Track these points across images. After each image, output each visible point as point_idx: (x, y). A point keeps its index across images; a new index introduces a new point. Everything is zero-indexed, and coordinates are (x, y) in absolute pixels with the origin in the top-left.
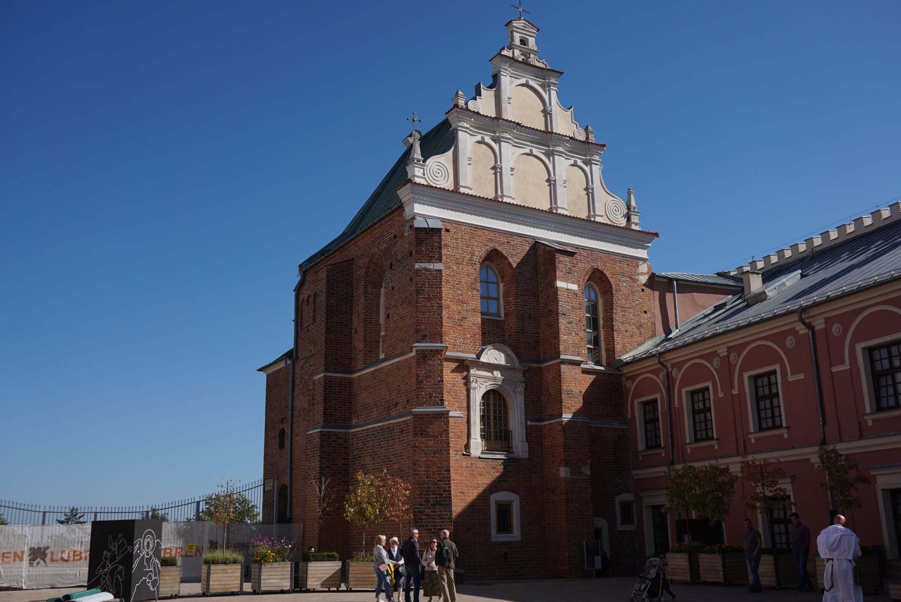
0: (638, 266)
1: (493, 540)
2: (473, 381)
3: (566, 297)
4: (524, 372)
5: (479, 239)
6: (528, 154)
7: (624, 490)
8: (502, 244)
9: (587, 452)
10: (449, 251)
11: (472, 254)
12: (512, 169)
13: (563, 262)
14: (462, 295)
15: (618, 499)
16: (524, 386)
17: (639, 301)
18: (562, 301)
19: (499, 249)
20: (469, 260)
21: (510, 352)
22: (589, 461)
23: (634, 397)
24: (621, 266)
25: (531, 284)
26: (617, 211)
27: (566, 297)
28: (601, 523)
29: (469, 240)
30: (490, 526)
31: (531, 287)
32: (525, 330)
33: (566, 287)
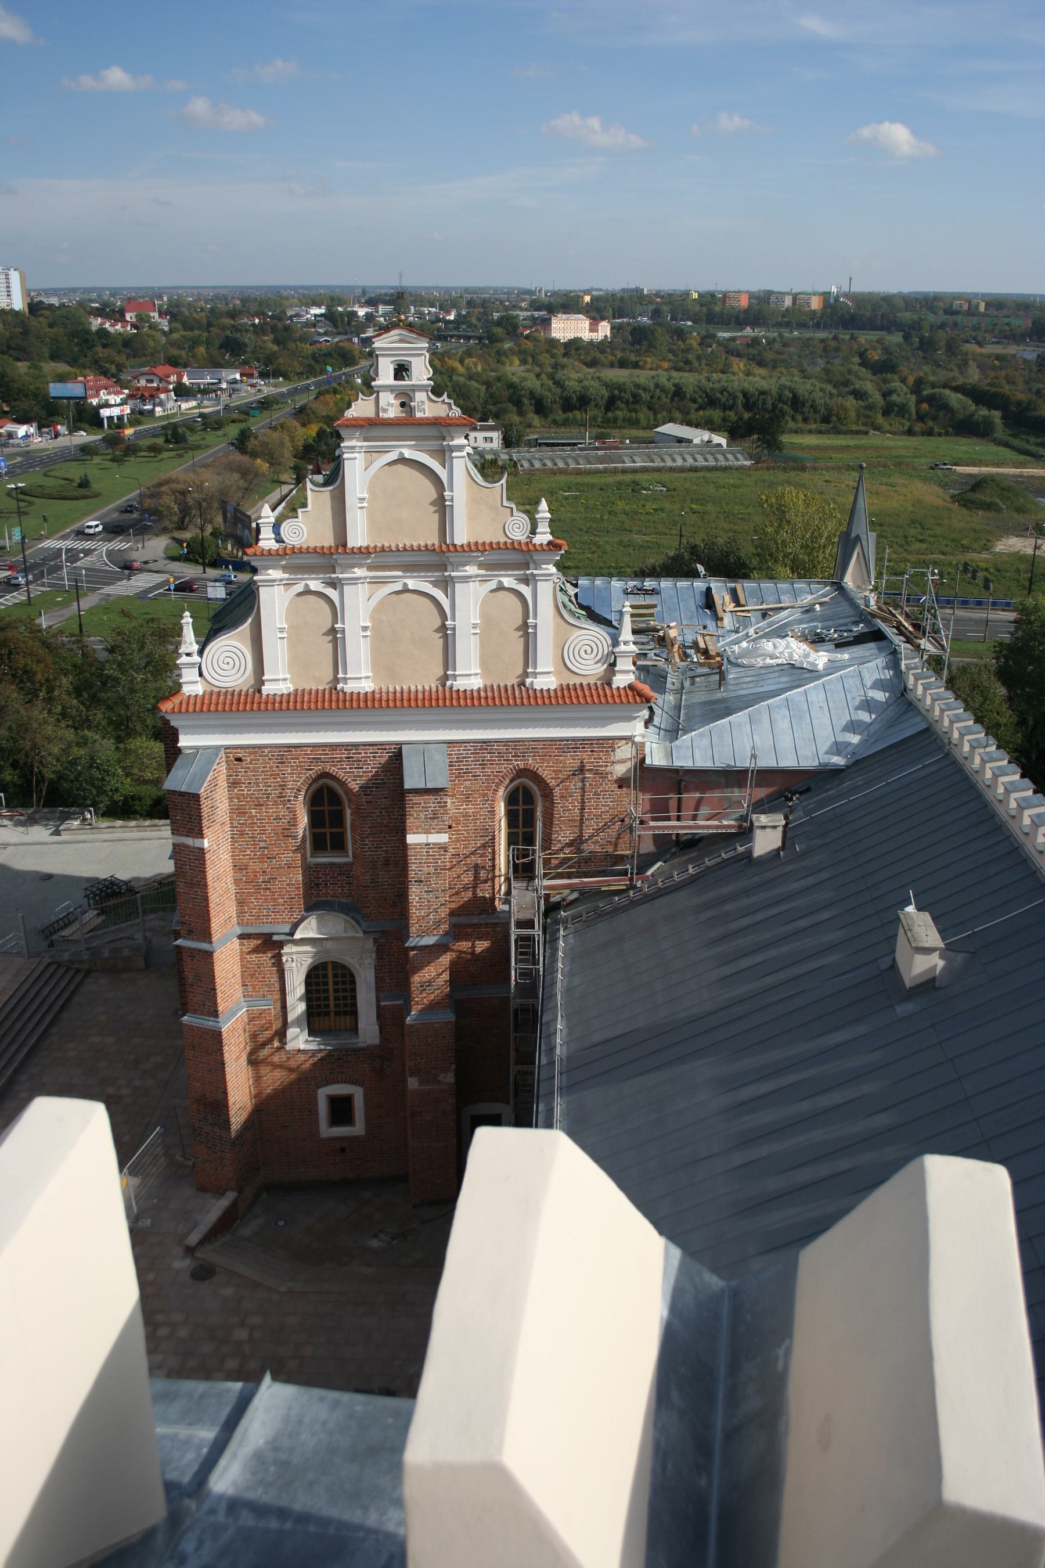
0: (613, 751)
2: (287, 961)
5: (295, 762)
6: (398, 593)
8: (337, 762)
10: (243, 790)
11: (283, 787)
13: (420, 804)
14: (267, 848)
17: (609, 805)
18: (416, 863)
19: (333, 770)
20: (278, 797)
22: (453, 1067)
24: (577, 756)
25: (388, 816)
26: (589, 651)
29: (277, 767)
30: (318, 1121)
31: (390, 819)
32: (377, 882)
33: (425, 841)
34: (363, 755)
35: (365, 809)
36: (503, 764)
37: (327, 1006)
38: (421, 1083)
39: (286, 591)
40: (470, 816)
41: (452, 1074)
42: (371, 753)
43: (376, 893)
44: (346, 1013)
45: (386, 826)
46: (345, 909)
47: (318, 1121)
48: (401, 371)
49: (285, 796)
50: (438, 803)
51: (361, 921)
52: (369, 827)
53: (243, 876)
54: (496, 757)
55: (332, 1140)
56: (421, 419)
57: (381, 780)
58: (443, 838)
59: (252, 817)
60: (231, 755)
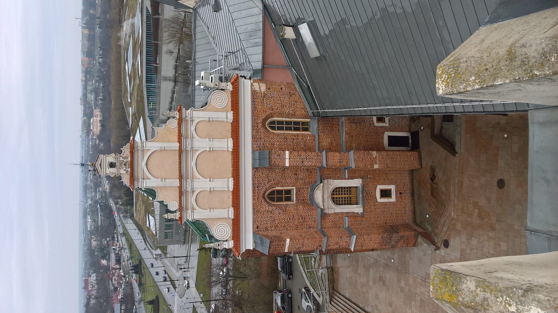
1: (395, 201)
3: (293, 160)
7: (372, 120)
8: (259, 191)
9: (367, 153)
10: (269, 226)
13: (274, 161)
14: (290, 218)
15: (376, 124)
16: (330, 180)
18: (296, 163)
19: (262, 193)
20: (271, 213)
22: (370, 152)
25: (279, 173)
27: (293, 160)
33: (288, 159)
34: (256, 182)
35: (276, 181)
36: (260, 131)
37: (347, 198)
38: (376, 164)
39: (196, 210)
40: (279, 143)
41: (373, 152)
42: (256, 179)
43: (307, 178)
44: (350, 191)
45: (283, 174)
46: (313, 190)
47: (389, 202)
48: (112, 165)
49: (271, 210)
50: (274, 154)
51: (317, 184)
52: (283, 181)
53: (300, 226)
54: (258, 133)
55: (396, 198)
56: (131, 158)
57: (265, 175)
59: (278, 223)
60: (256, 230)
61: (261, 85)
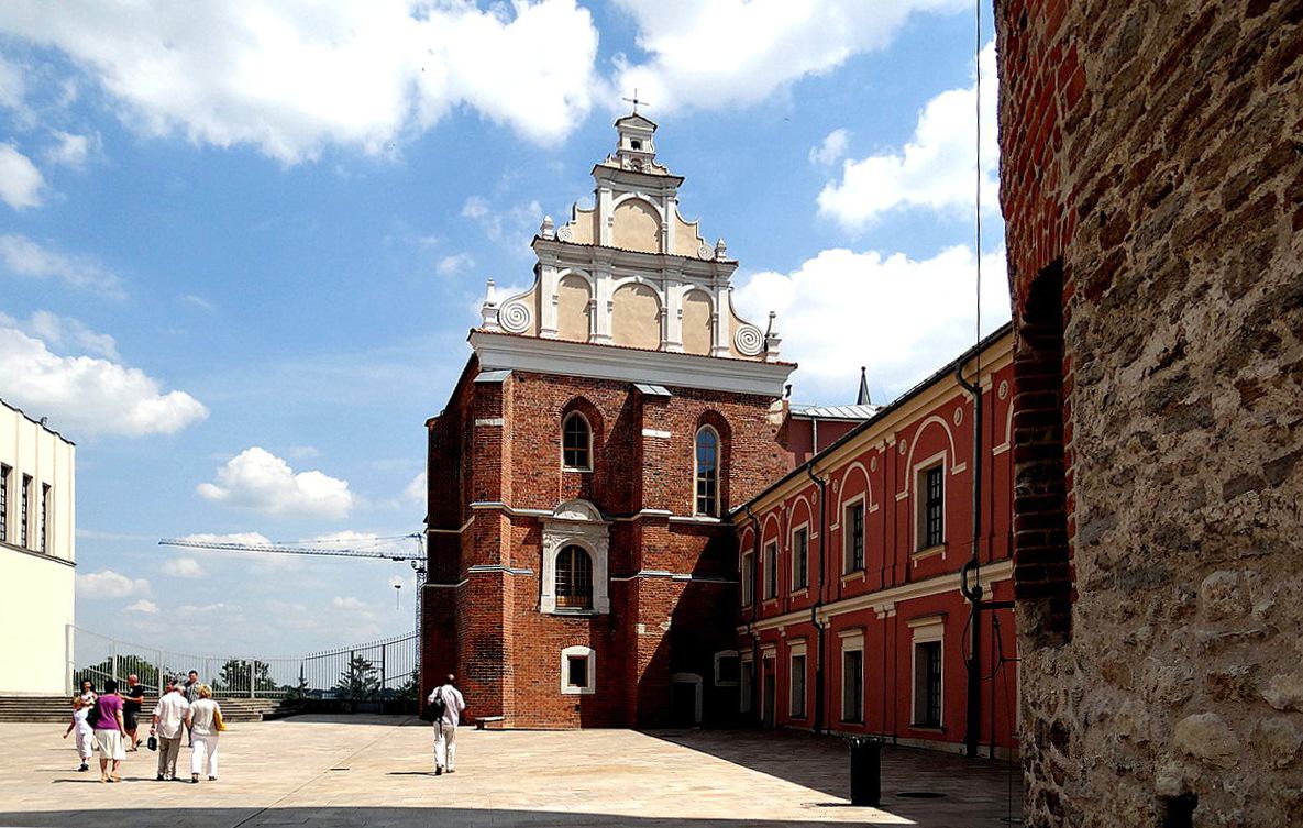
4: (610, 528)
12: (610, 304)
15: (717, 656)
21: (592, 506)
22: (670, 618)
23: (743, 551)
28: (697, 680)
38: (646, 630)
58: (667, 435)
61: (780, 415)
